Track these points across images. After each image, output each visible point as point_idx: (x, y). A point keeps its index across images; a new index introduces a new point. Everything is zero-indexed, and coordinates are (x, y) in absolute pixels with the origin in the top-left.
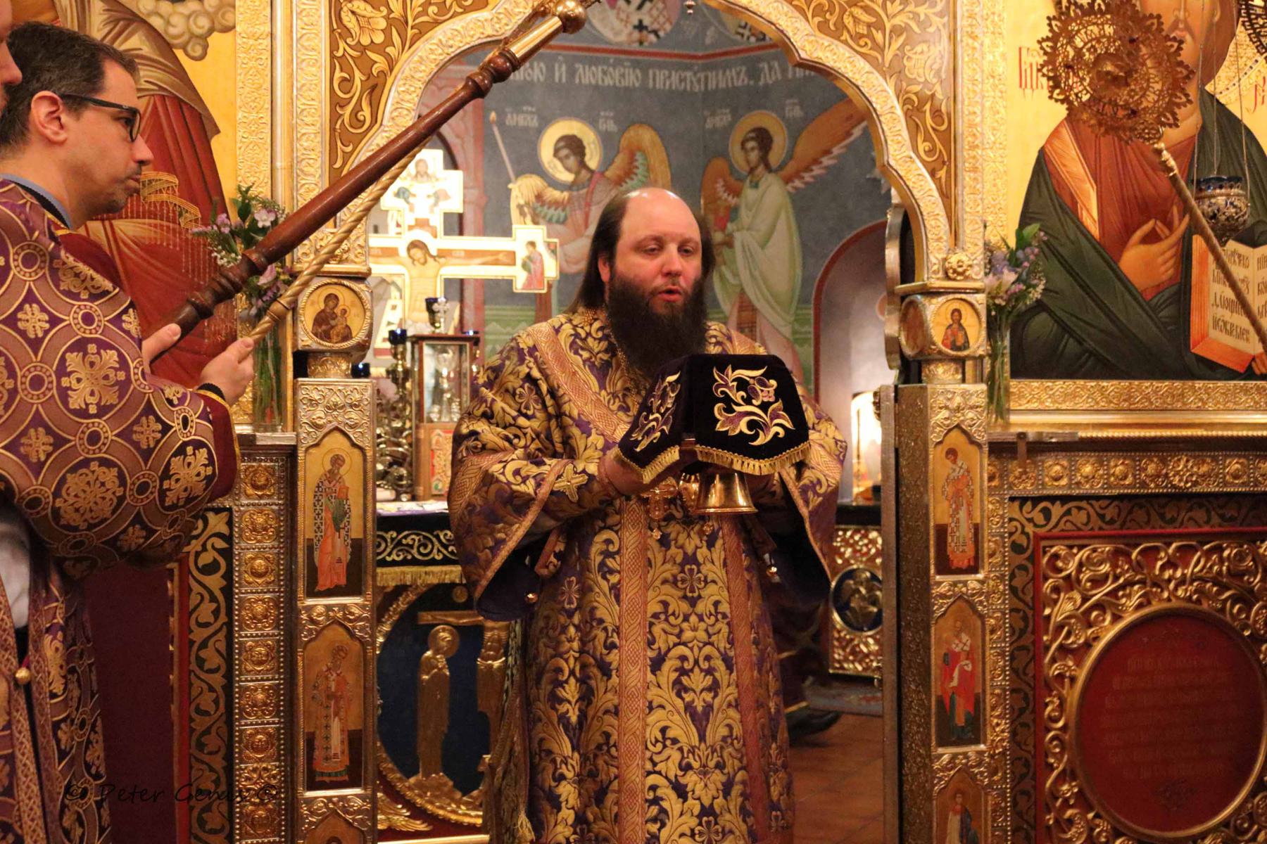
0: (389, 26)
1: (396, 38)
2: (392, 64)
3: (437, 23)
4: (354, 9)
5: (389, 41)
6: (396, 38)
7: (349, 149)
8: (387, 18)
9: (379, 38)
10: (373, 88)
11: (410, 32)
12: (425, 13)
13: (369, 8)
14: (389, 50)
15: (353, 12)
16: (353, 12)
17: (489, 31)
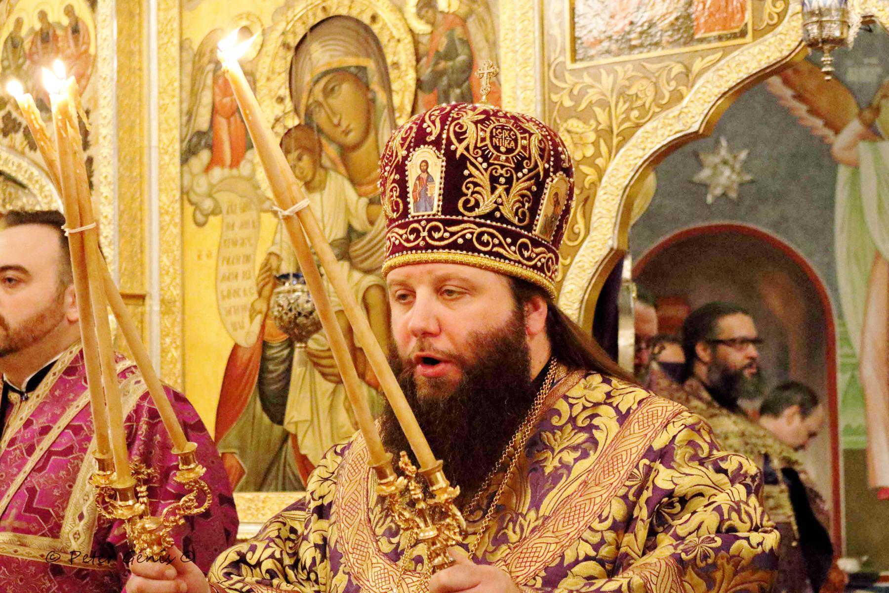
0: (598, 137)
1: (604, 149)
2: (600, 173)
3: (638, 126)
4: (569, 128)
5: (598, 154)
6: (604, 149)
7: (567, 262)
8: (596, 131)
9: (590, 151)
10: (586, 200)
11: (615, 141)
12: (627, 119)
13: (581, 124)
14: (600, 161)
15: (569, 132)
16: (569, 132)
17: (678, 127)
